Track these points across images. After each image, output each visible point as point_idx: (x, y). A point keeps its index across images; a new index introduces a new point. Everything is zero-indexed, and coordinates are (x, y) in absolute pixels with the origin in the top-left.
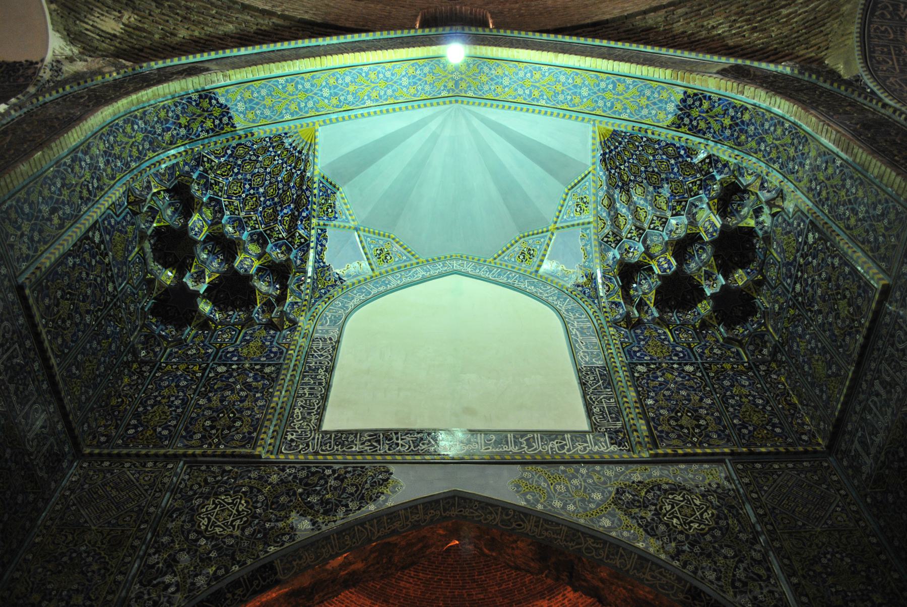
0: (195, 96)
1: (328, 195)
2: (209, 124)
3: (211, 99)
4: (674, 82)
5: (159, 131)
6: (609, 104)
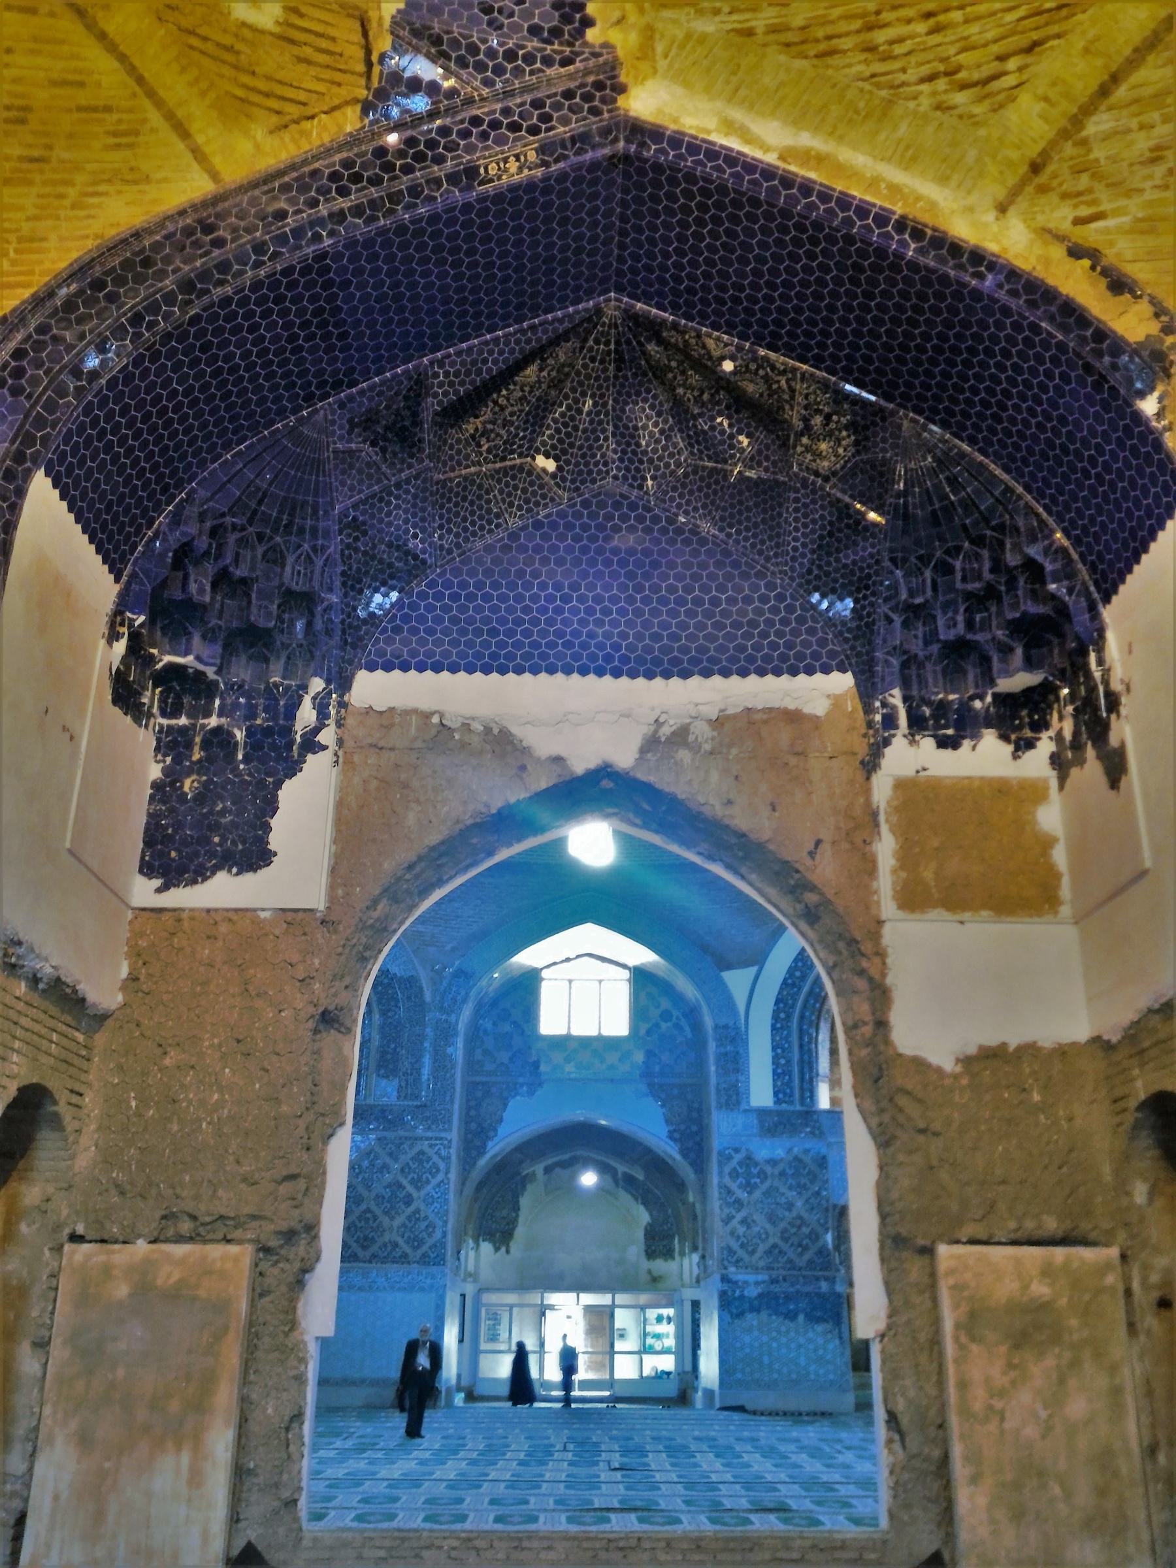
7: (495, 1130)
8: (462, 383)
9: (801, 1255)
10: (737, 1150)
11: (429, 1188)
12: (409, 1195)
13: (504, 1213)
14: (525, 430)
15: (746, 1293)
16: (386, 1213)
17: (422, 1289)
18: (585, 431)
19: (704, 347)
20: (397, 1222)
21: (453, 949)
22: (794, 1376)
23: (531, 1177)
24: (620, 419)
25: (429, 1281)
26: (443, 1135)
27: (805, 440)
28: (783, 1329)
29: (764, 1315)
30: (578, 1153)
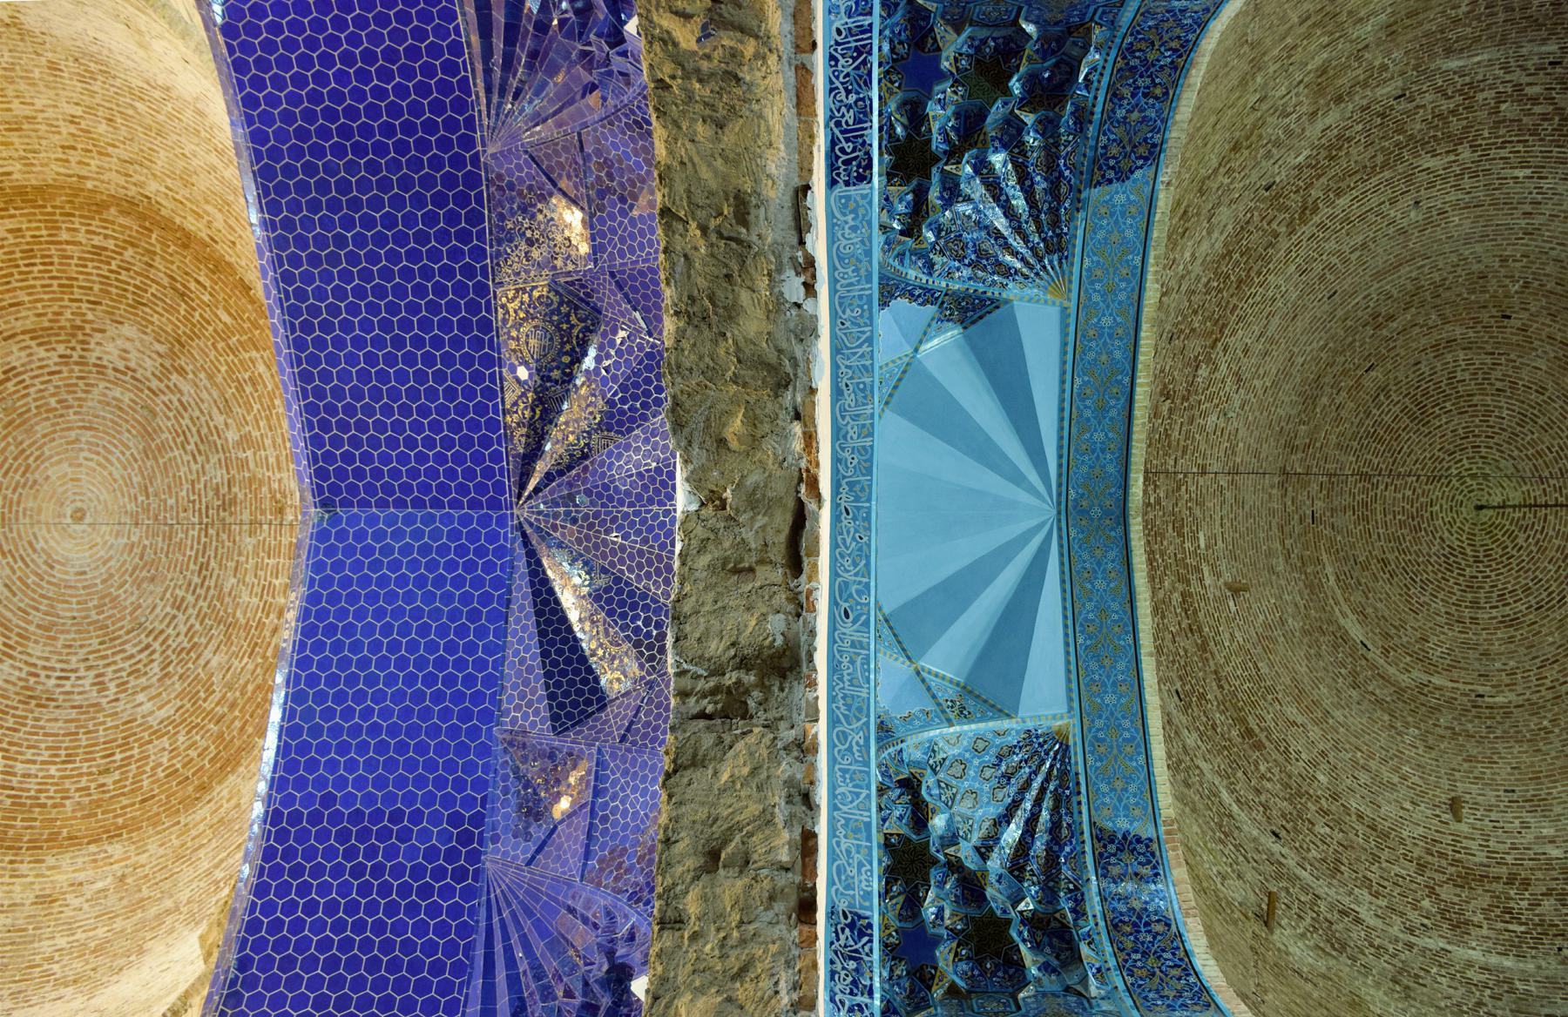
0: (1157, 138)
1: (966, 310)
2: (1114, 150)
3: (1146, 159)
4: (1160, 822)
5: (1140, 82)
6: (1101, 735)
8: (533, 692)
14: (636, 618)
18: (645, 541)
19: (515, 404)
24: (639, 497)
27: (559, 263)
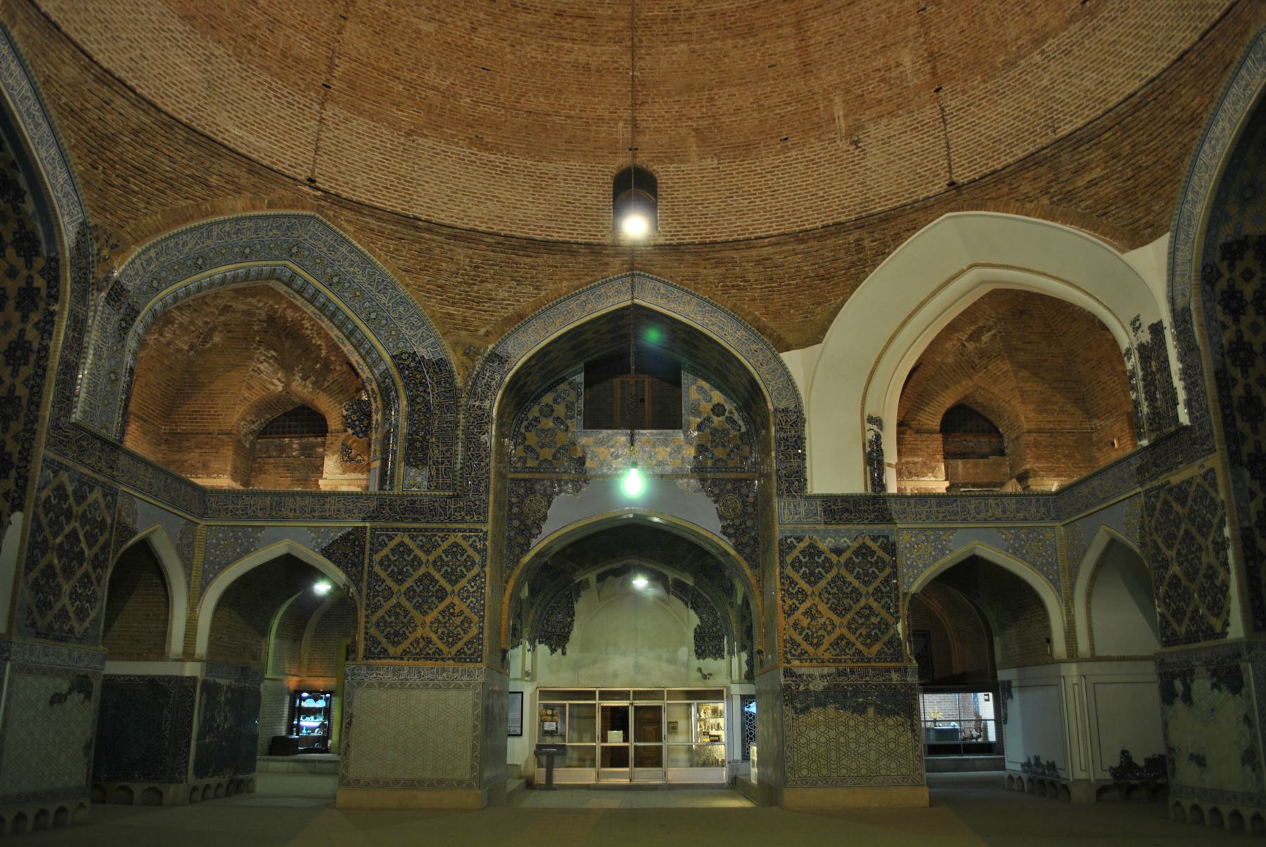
7: (539, 528)
9: (869, 646)
10: (800, 539)
11: (464, 582)
12: (443, 589)
13: (560, 617)
15: (811, 687)
16: (417, 607)
17: (459, 687)
20: (429, 619)
21: (487, 334)
22: (864, 772)
23: (584, 585)
25: (465, 678)
26: (478, 526)
28: (852, 723)
29: (831, 709)
30: (629, 561)
